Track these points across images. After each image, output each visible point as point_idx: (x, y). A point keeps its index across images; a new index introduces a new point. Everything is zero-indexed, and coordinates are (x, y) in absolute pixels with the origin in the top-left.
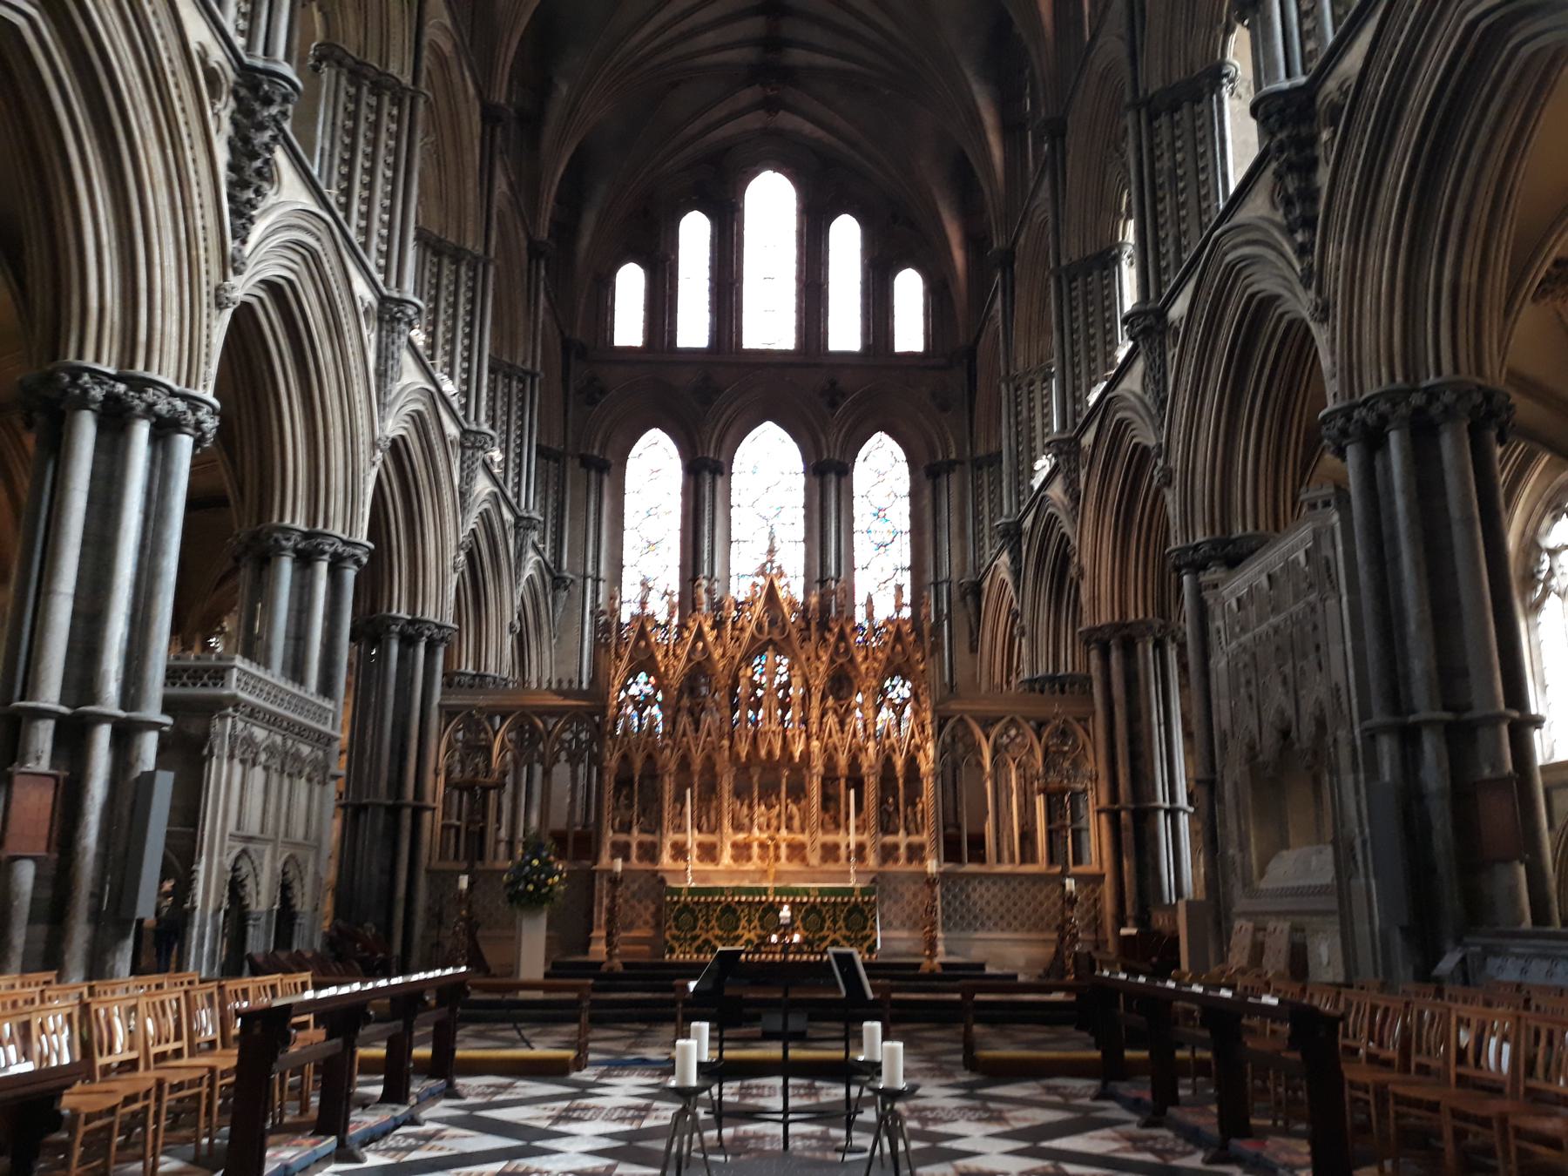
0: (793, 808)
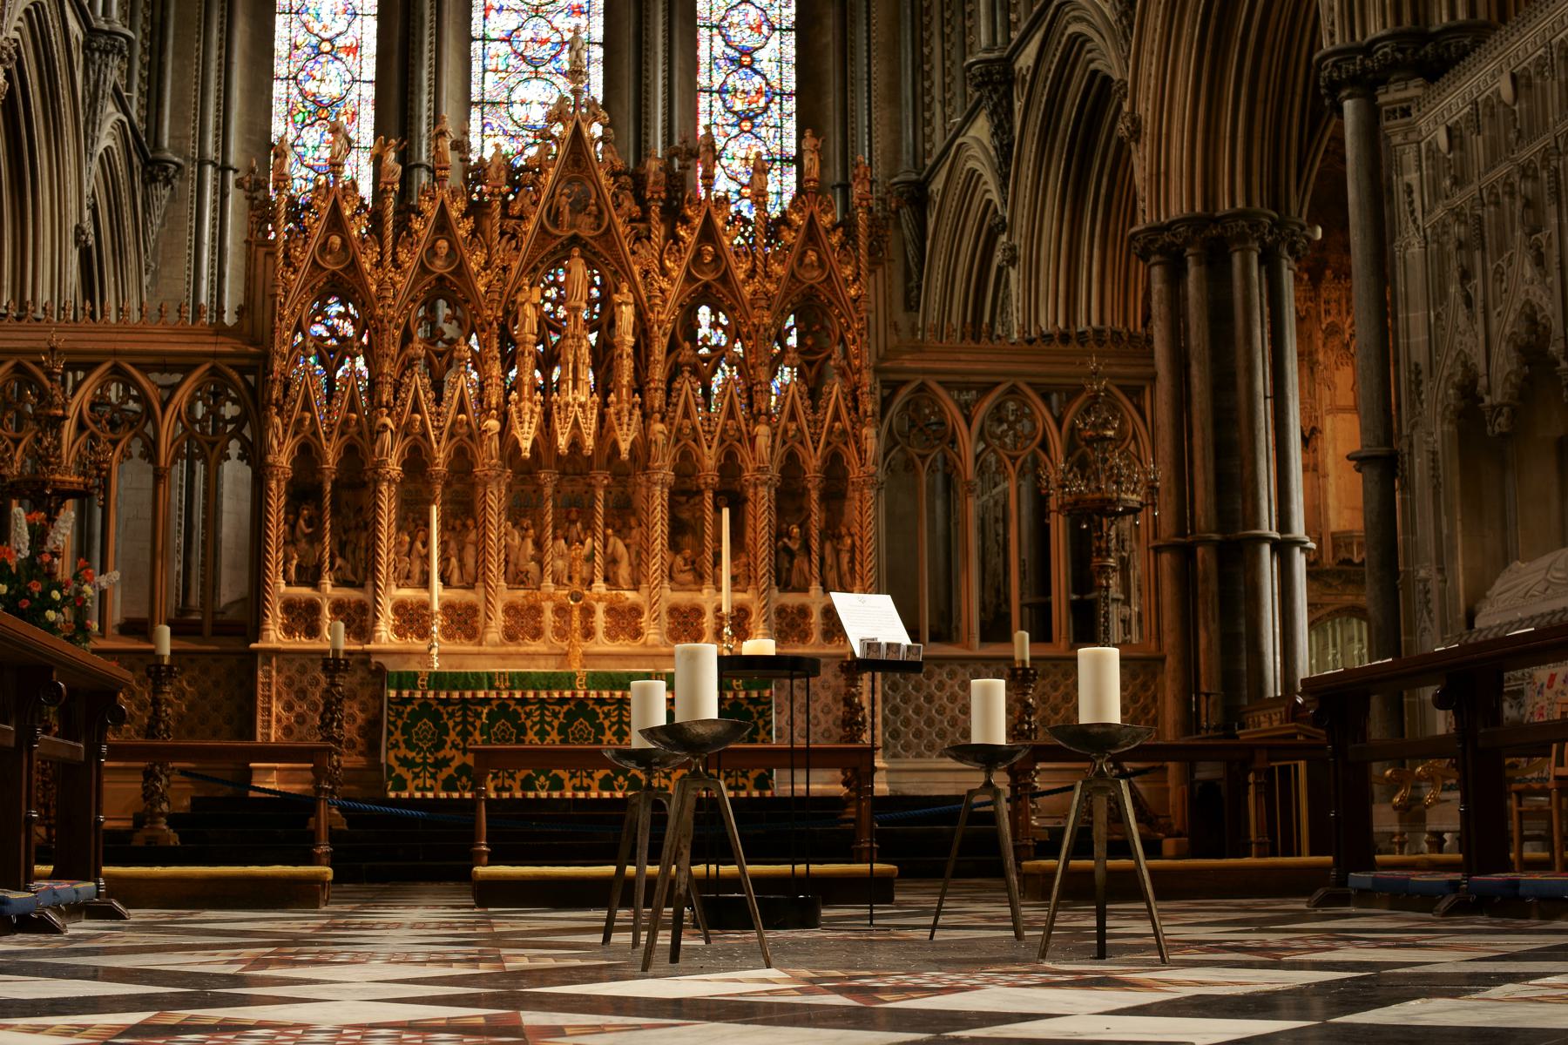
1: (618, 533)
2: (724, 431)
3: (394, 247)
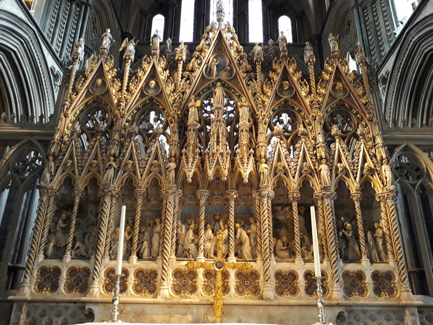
0: (243, 233)
1: (243, 227)
2: (301, 169)
3: (128, 83)
